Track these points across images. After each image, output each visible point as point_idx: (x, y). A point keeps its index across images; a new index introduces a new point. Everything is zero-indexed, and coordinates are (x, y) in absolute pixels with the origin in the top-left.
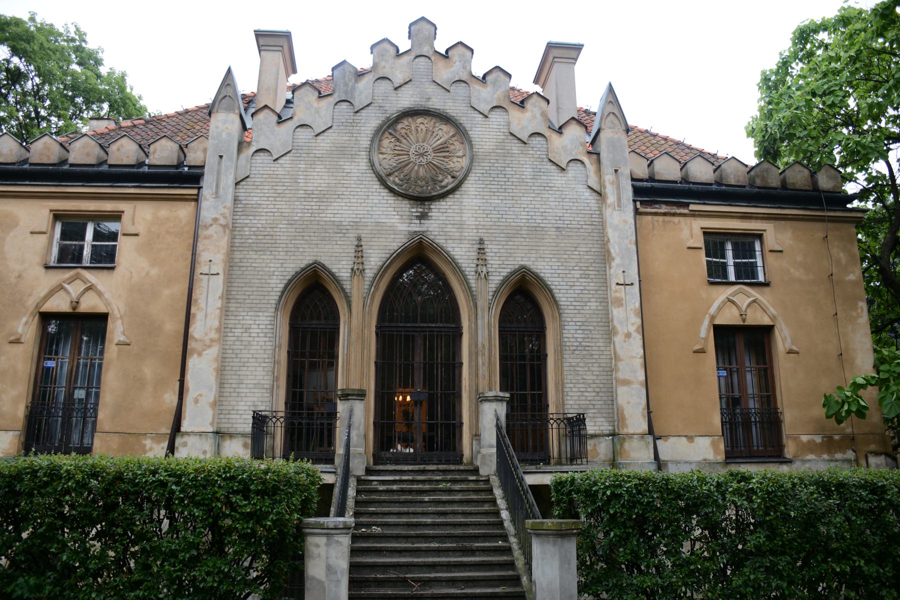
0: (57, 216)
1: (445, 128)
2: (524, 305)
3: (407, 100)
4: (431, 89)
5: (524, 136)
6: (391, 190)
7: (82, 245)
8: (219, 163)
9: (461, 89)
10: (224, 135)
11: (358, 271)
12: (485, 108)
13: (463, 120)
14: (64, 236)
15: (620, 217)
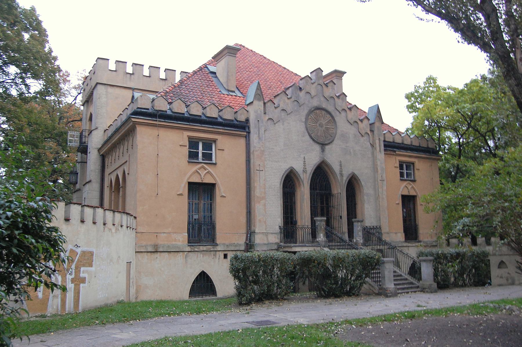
0: (190, 138)
1: (328, 116)
2: (352, 186)
3: (315, 103)
4: (322, 99)
5: (352, 122)
6: (314, 140)
7: (199, 152)
8: (259, 123)
9: (331, 101)
10: (259, 112)
11: (305, 171)
12: (340, 109)
13: (333, 114)
14: (190, 147)
15: (381, 155)
